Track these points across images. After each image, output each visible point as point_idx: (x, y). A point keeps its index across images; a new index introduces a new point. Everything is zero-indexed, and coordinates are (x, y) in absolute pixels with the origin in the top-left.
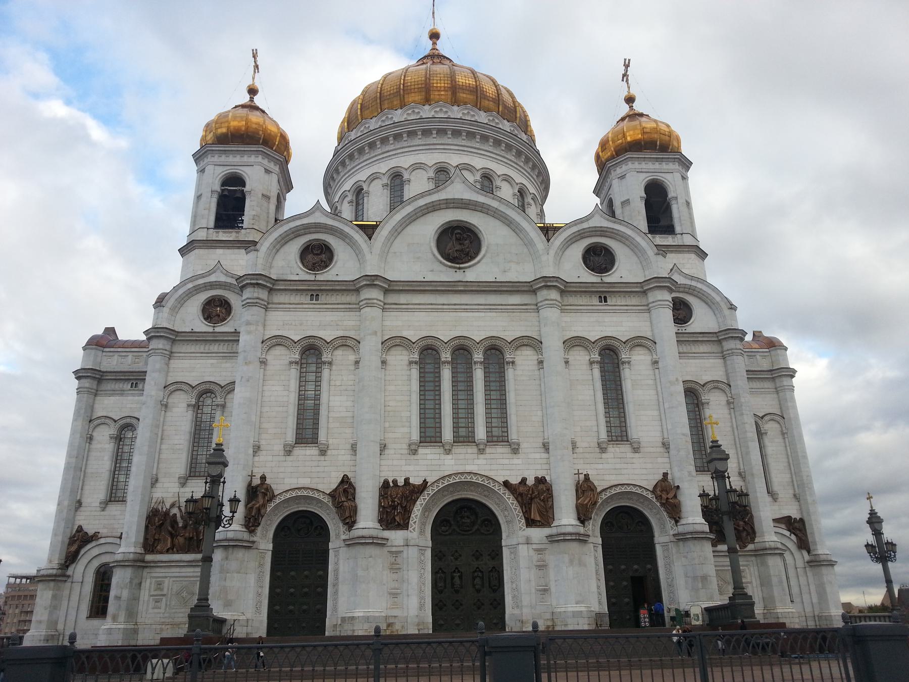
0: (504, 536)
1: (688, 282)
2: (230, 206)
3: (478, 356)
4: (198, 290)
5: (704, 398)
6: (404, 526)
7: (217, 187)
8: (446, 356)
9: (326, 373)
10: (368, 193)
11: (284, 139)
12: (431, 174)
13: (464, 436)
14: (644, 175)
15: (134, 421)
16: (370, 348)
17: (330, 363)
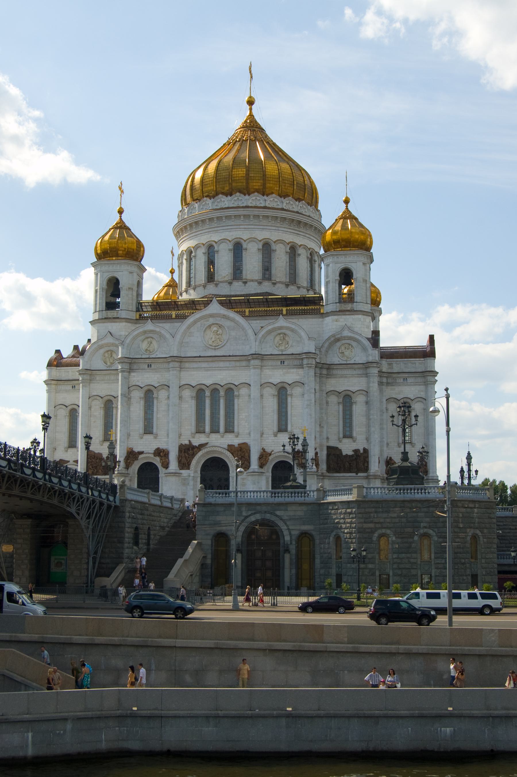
0: (230, 472)
1: (353, 335)
2: (111, 294)
3: (222, 393)
4: (101, 347)
5: (354, 400)
6: (188, 468)
7: (105, 286)
8: (208, 393)
9: (155, 401)
10: (195, 256)
11: (139, 245)
12: (231, 246)
13: (215, 430)
14: (339, 265)
15: (76, 407)
16: (174, 390)
17: (157, 398)
